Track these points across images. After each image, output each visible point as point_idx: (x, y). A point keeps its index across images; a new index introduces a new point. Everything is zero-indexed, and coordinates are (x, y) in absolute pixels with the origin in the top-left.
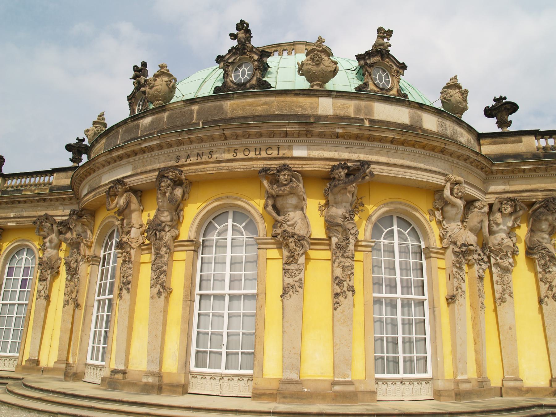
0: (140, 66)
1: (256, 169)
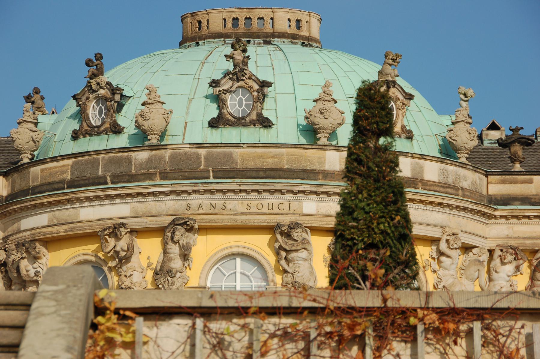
1: (269, 224)
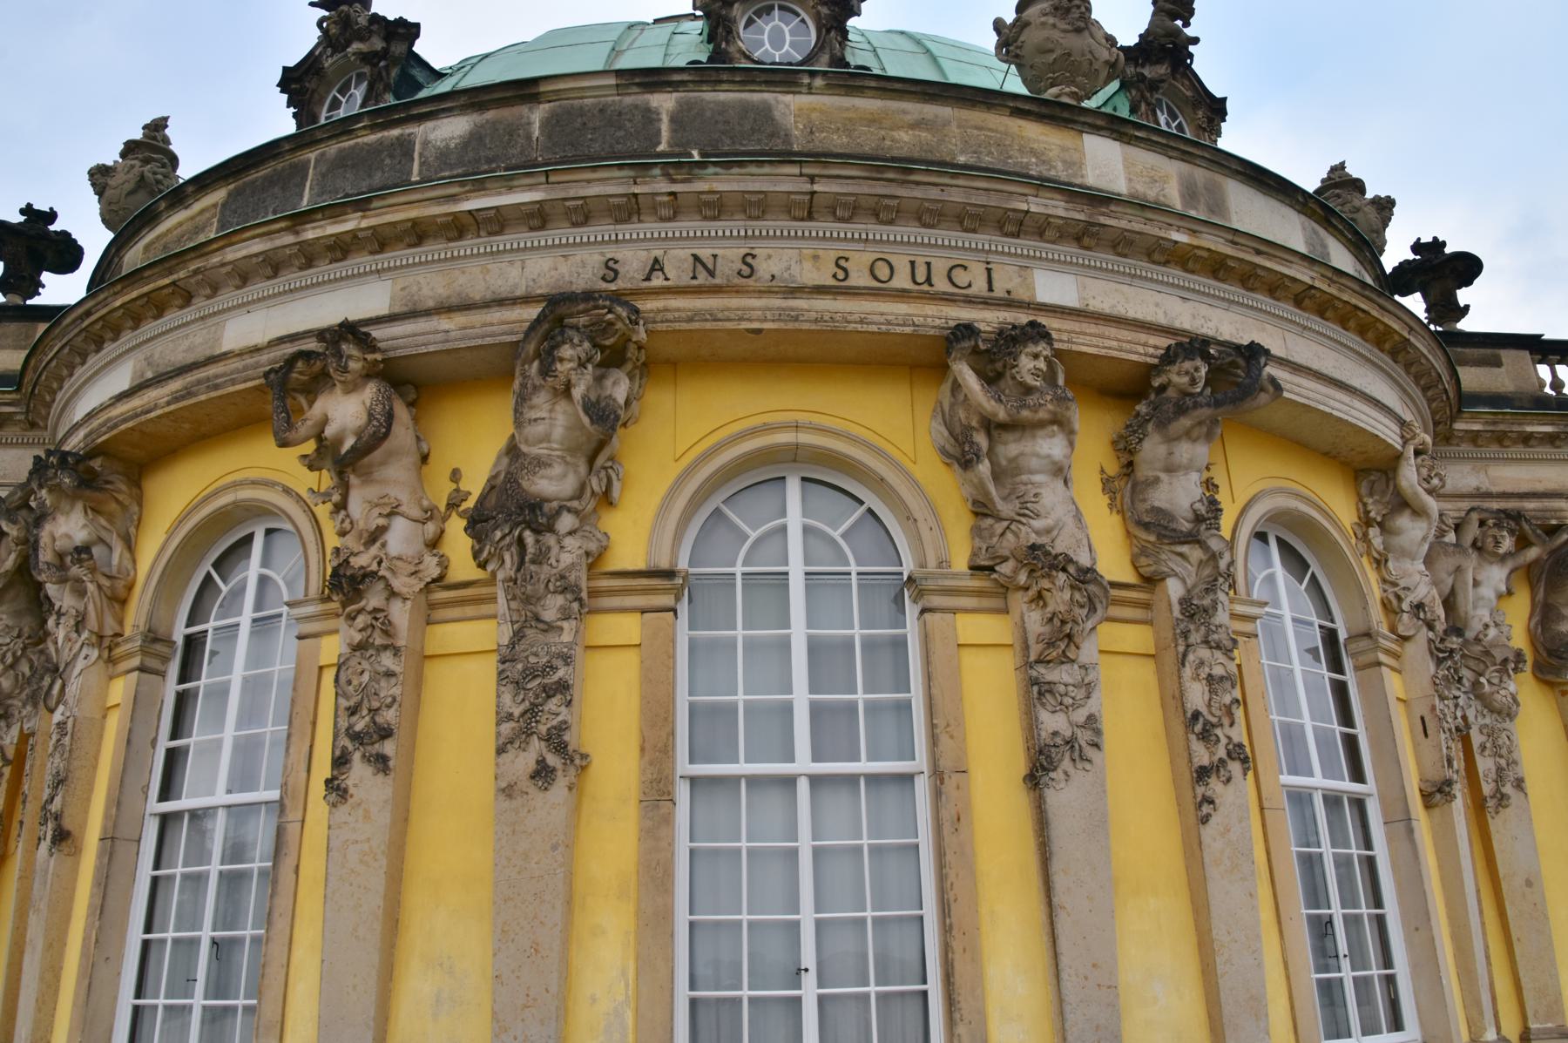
1: (922, 331)
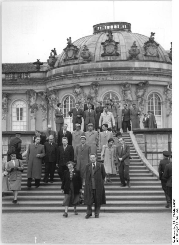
0: (69, 39)
